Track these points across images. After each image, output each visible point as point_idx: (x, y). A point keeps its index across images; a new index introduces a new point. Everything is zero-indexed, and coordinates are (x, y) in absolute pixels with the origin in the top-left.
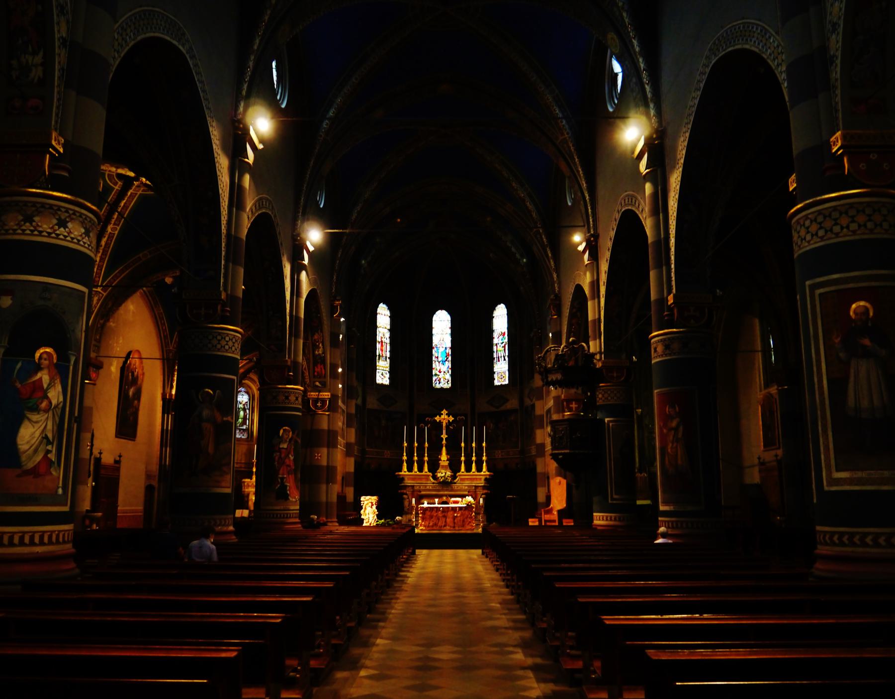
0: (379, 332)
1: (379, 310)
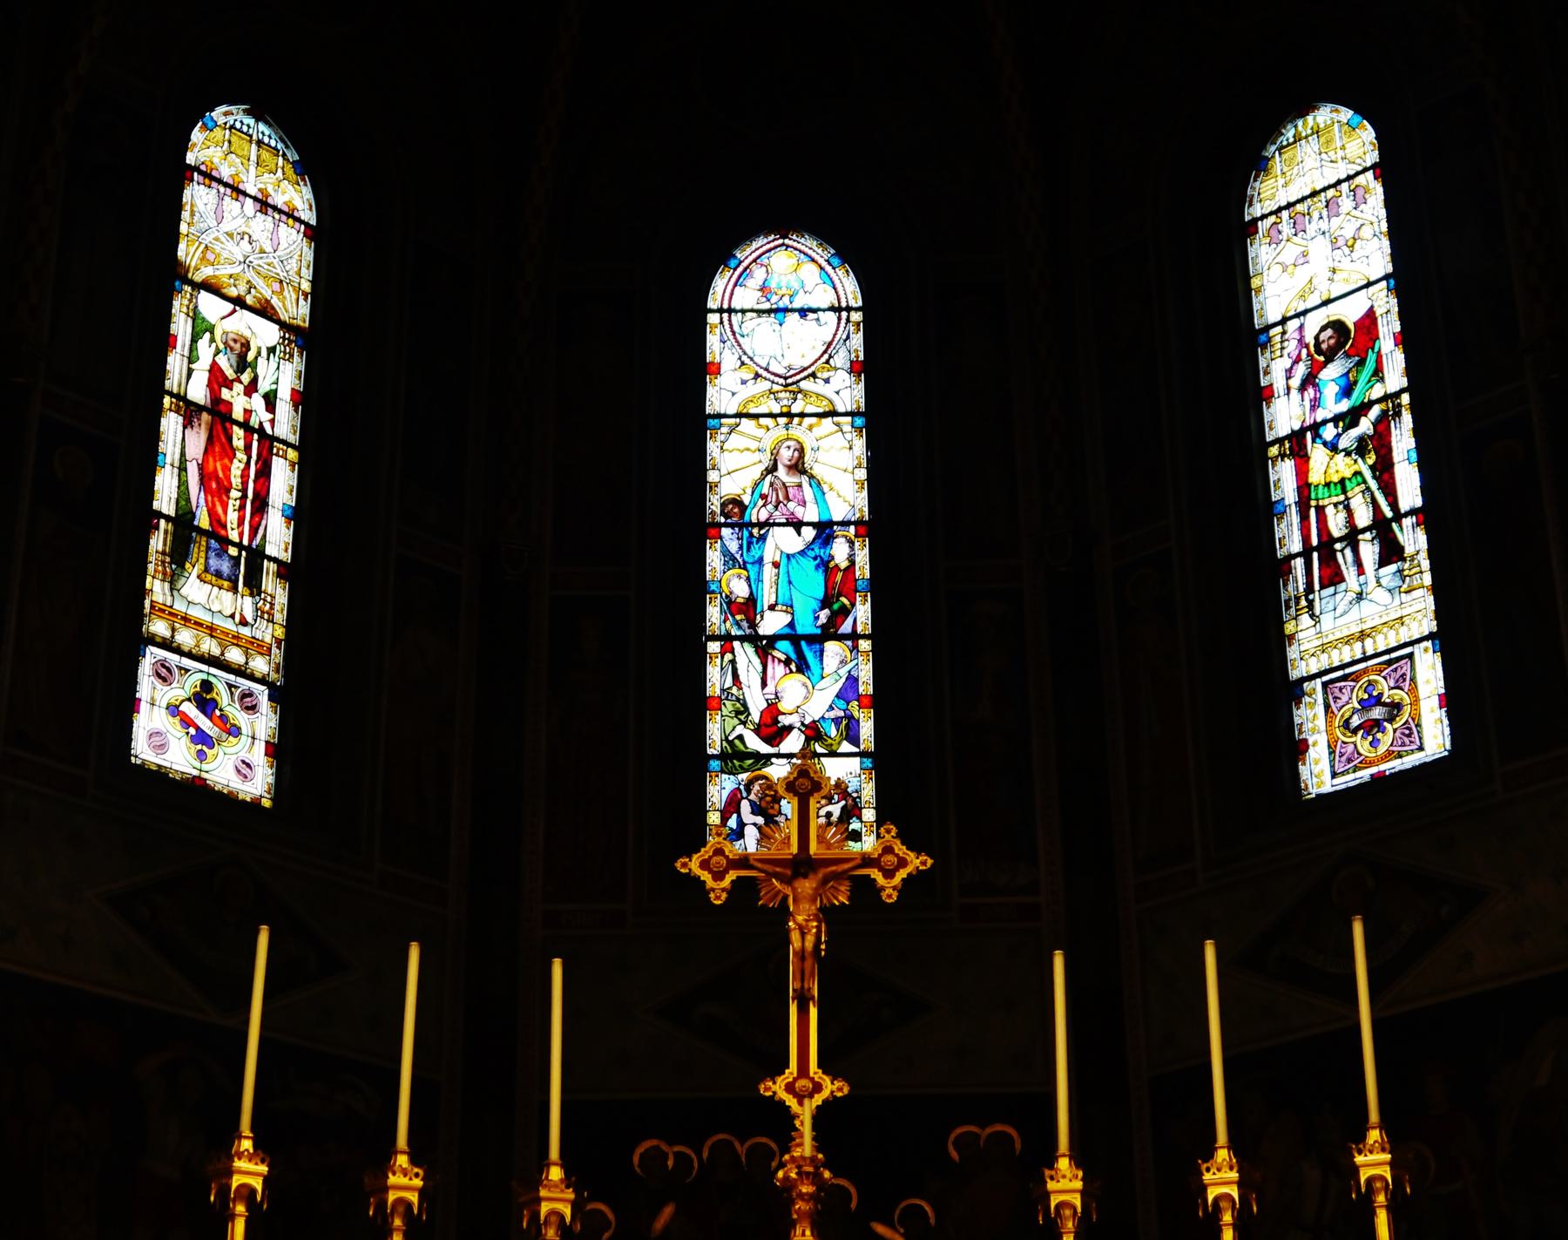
0: (201, 327)
1: (203, 147)
